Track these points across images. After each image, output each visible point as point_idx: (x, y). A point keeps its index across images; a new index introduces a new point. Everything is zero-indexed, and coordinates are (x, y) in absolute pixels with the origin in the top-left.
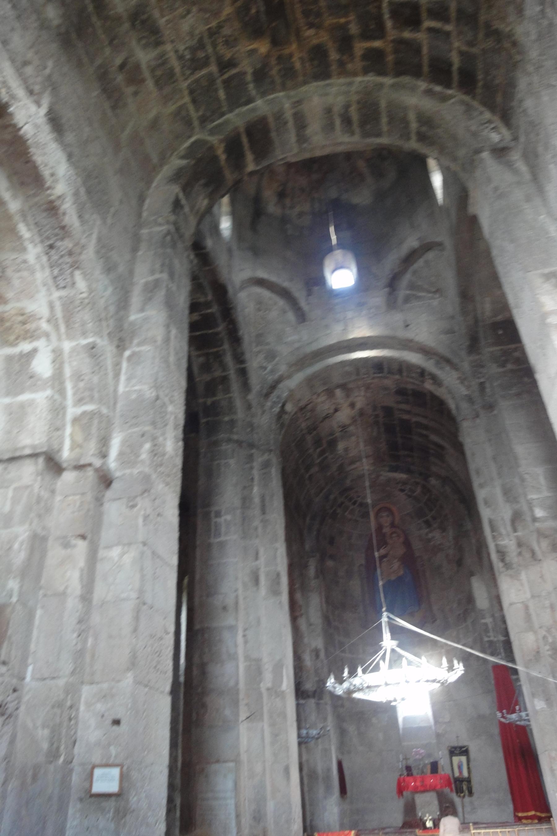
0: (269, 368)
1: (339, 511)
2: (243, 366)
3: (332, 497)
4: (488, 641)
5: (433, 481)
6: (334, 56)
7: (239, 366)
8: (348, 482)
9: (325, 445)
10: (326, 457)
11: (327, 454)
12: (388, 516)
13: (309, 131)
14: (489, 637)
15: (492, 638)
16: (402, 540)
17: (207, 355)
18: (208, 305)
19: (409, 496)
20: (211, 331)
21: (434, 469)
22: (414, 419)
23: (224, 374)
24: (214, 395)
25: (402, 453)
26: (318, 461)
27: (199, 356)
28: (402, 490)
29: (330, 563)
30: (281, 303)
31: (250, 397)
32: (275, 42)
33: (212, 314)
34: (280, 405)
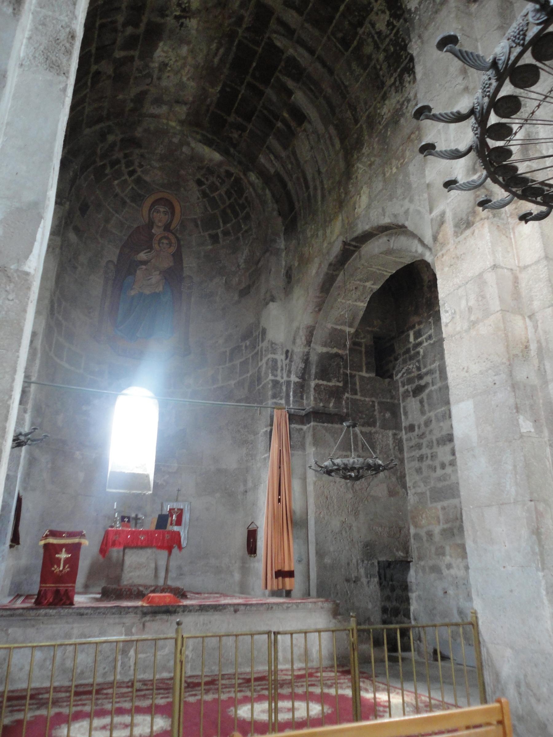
1: (108, 171)
3: (111, 138)
4: (272, 381)
5: (253, 177)
8: (139, 133)
9: (143, 26)
10: (132, 59)
11: (136, 53)
12: (165, 213)
14: (276, 376)
15: (279, 378)
16: (173, 249)
19: (204, 194)
21: (262, 159)
22: (291, 51)
25: (232, 118)
26: (119, 54)
28: (199, 183)
29: (72, 237)
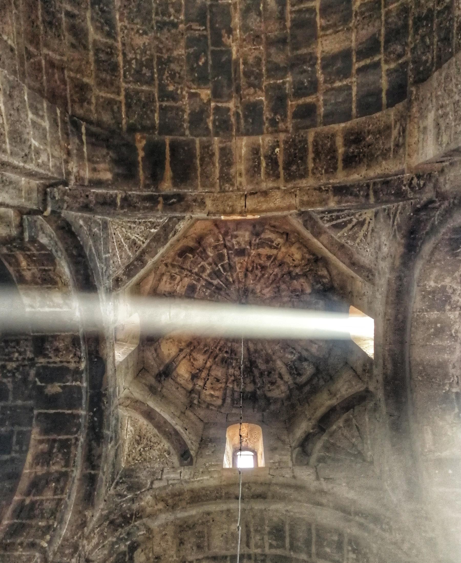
0: (129, 496)
2: (93, 472)
6: (267, 114)
7: (89, 471)
13: (232, 171)
17: (54, 441)
18: (77, 373)
20: (70, 412)
23: (64, 469)
24: (40, 492)
27: (41, 442)
30: (166, 444)
31: (88, 513)
32: (216, 95)
33: (79, 388)
34: (128, 543)
